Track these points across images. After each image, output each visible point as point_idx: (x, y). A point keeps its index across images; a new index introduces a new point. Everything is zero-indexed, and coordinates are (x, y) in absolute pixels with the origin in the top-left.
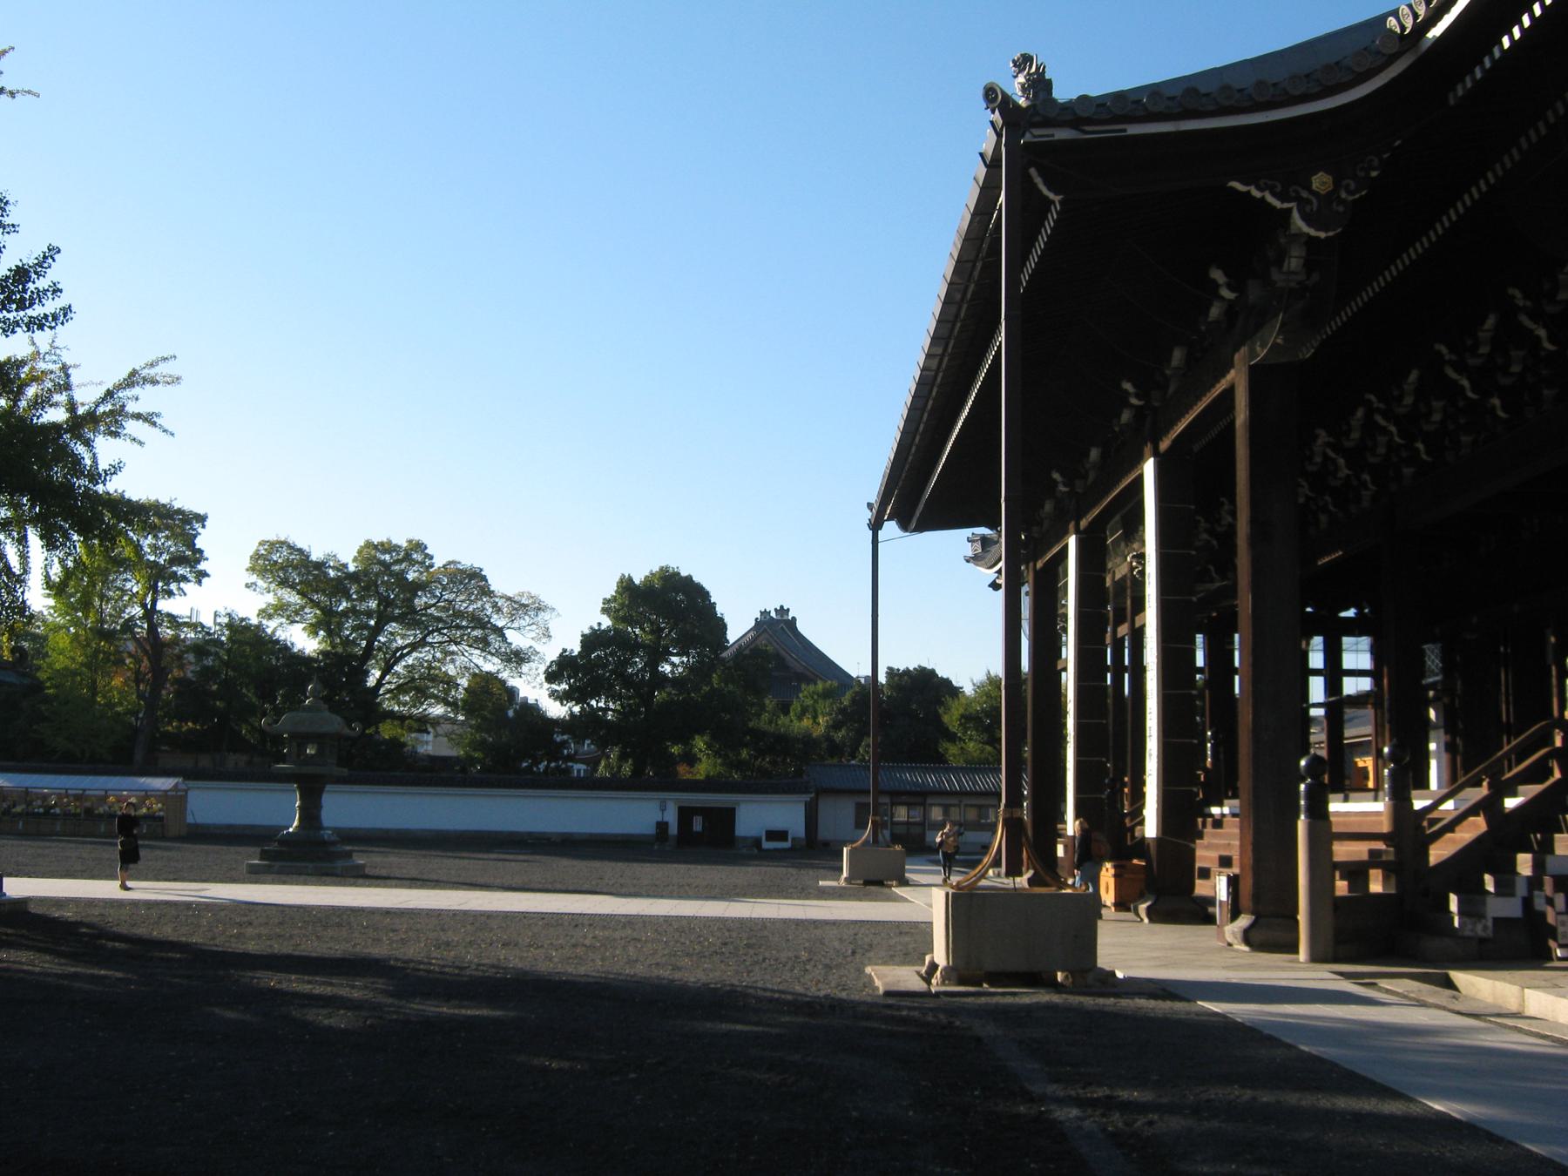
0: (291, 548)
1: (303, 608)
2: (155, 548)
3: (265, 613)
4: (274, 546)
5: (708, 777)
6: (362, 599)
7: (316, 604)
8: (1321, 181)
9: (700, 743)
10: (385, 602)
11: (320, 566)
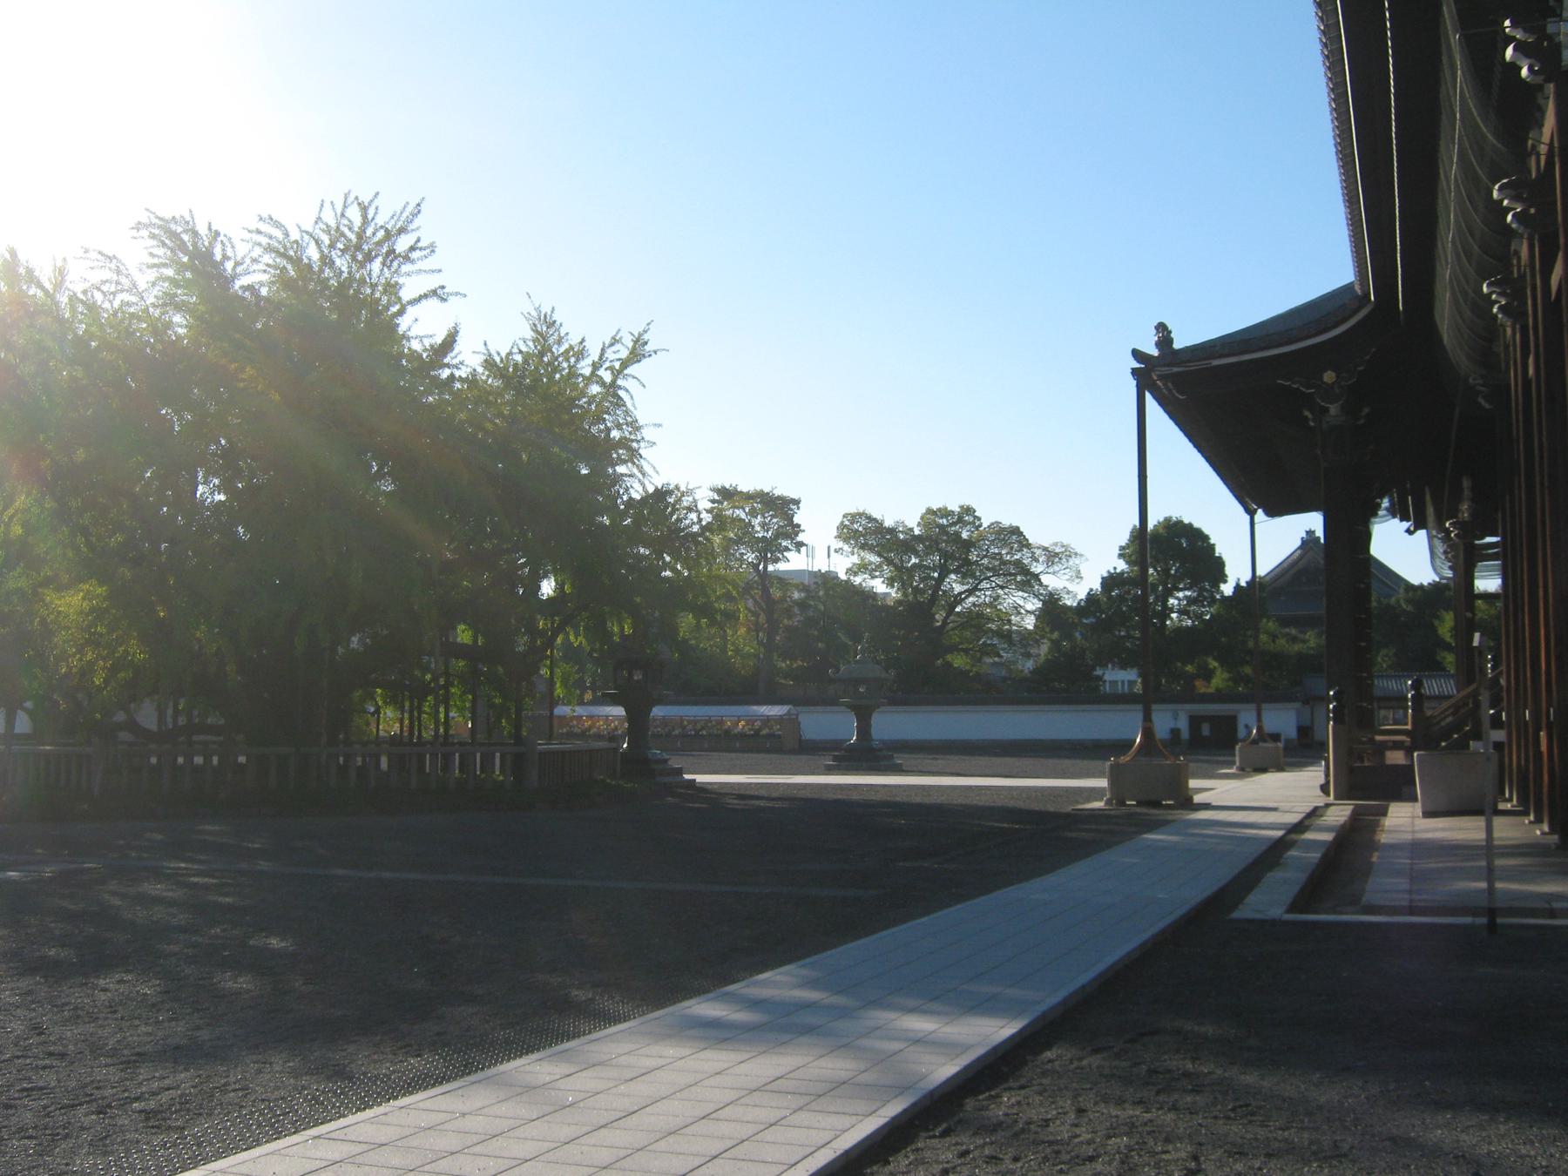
0: (870, 519)
1: (879, 567)
2: (763, 525)
3: (849, 571)
4: (854, 517)
5: (1218, 690)
6: (927, 554)
7: (889, 562)
8: (1329, 377)
9: (1214, 664)
10: (946, 555)
11: (892, 531)
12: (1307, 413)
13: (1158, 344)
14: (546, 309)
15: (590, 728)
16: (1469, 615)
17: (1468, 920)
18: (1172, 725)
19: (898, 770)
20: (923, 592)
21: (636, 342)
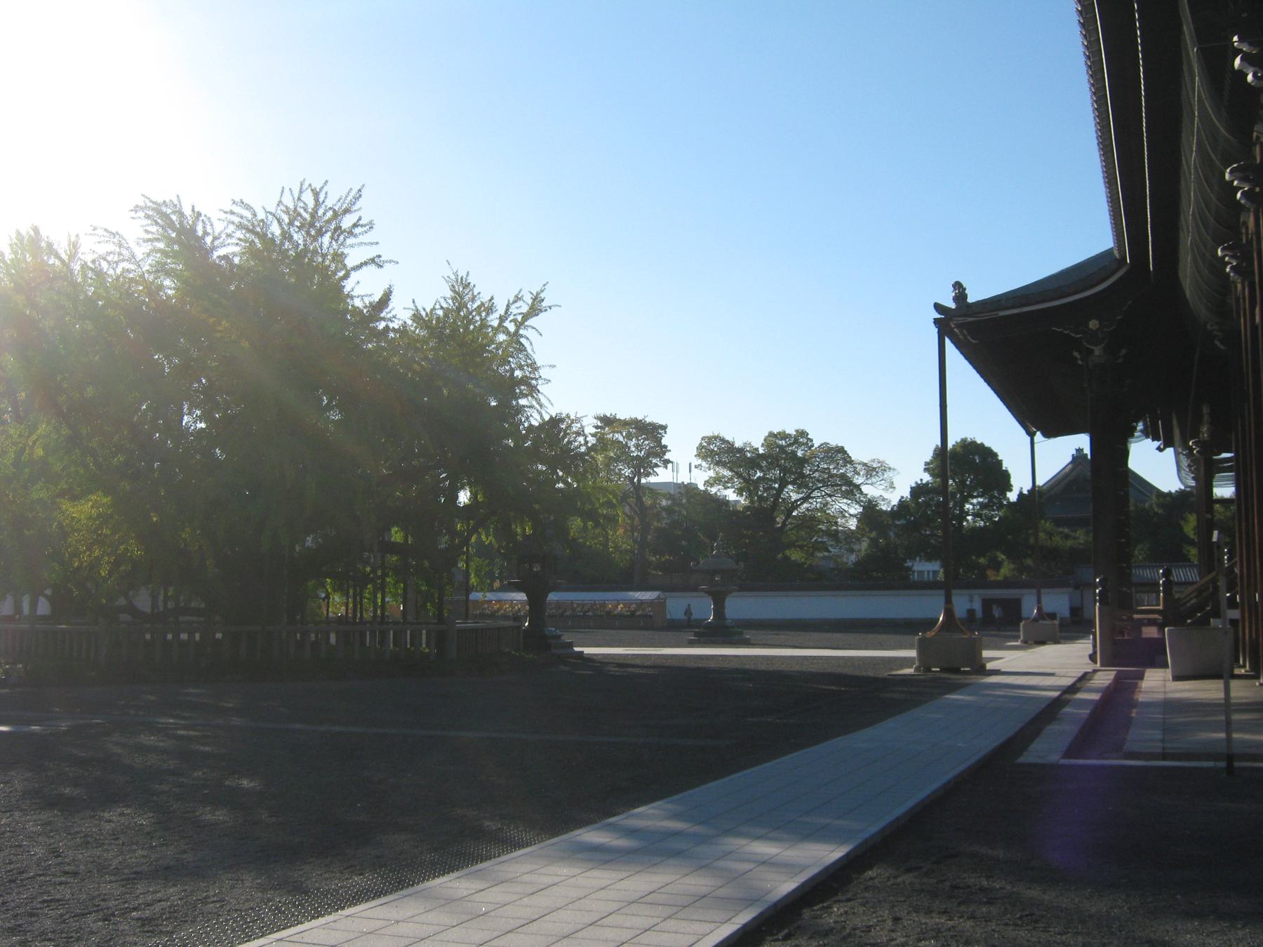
0: (723, 441)
1: (731, 479)
2: (637, 446)
3: (706, 483)
4: (710, 440)
5: (1006, 578)
6: (769, 469)
7: (739, 475)
8: (1093, 324)
10: (784, 470)
11: (741, 450)
12: (1076, 354)
13: (955, 299)
14: (462, 273)
15: (499, 610)
16: (1209, 516)
17: (1211, 764)
18: (968, 606)
19: (747, 643)
20: (767, 499)
21: (534, 299)
